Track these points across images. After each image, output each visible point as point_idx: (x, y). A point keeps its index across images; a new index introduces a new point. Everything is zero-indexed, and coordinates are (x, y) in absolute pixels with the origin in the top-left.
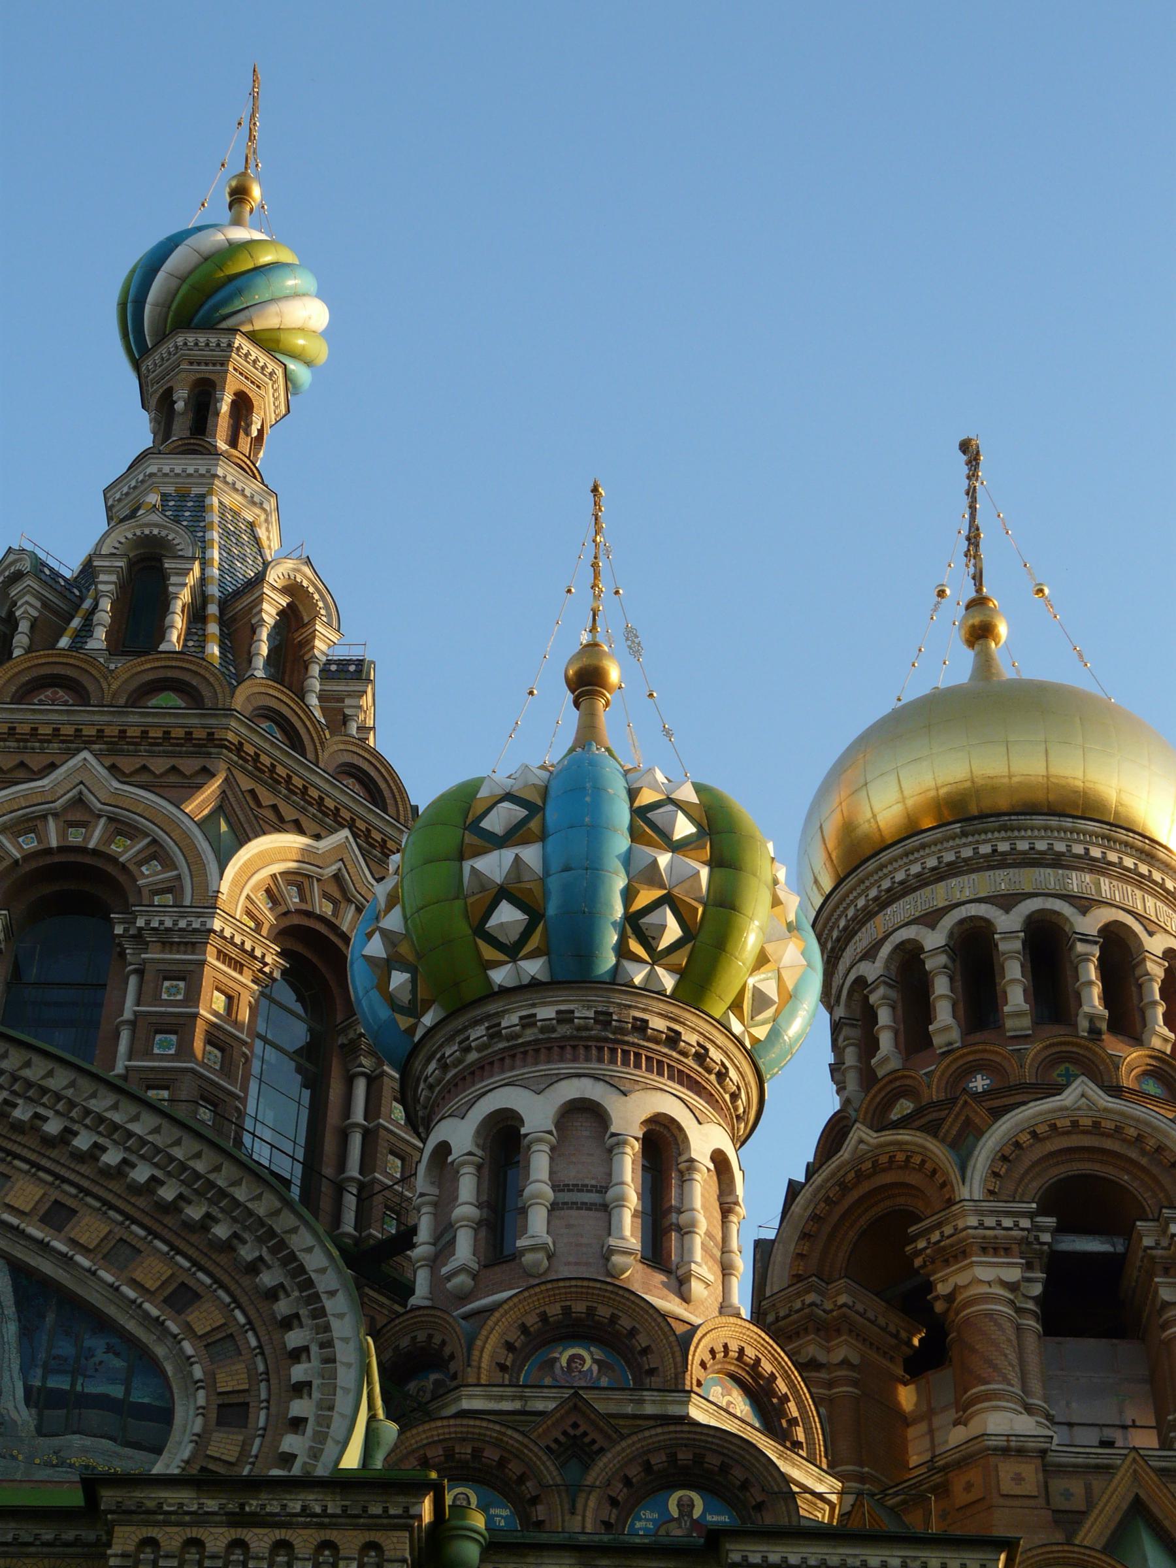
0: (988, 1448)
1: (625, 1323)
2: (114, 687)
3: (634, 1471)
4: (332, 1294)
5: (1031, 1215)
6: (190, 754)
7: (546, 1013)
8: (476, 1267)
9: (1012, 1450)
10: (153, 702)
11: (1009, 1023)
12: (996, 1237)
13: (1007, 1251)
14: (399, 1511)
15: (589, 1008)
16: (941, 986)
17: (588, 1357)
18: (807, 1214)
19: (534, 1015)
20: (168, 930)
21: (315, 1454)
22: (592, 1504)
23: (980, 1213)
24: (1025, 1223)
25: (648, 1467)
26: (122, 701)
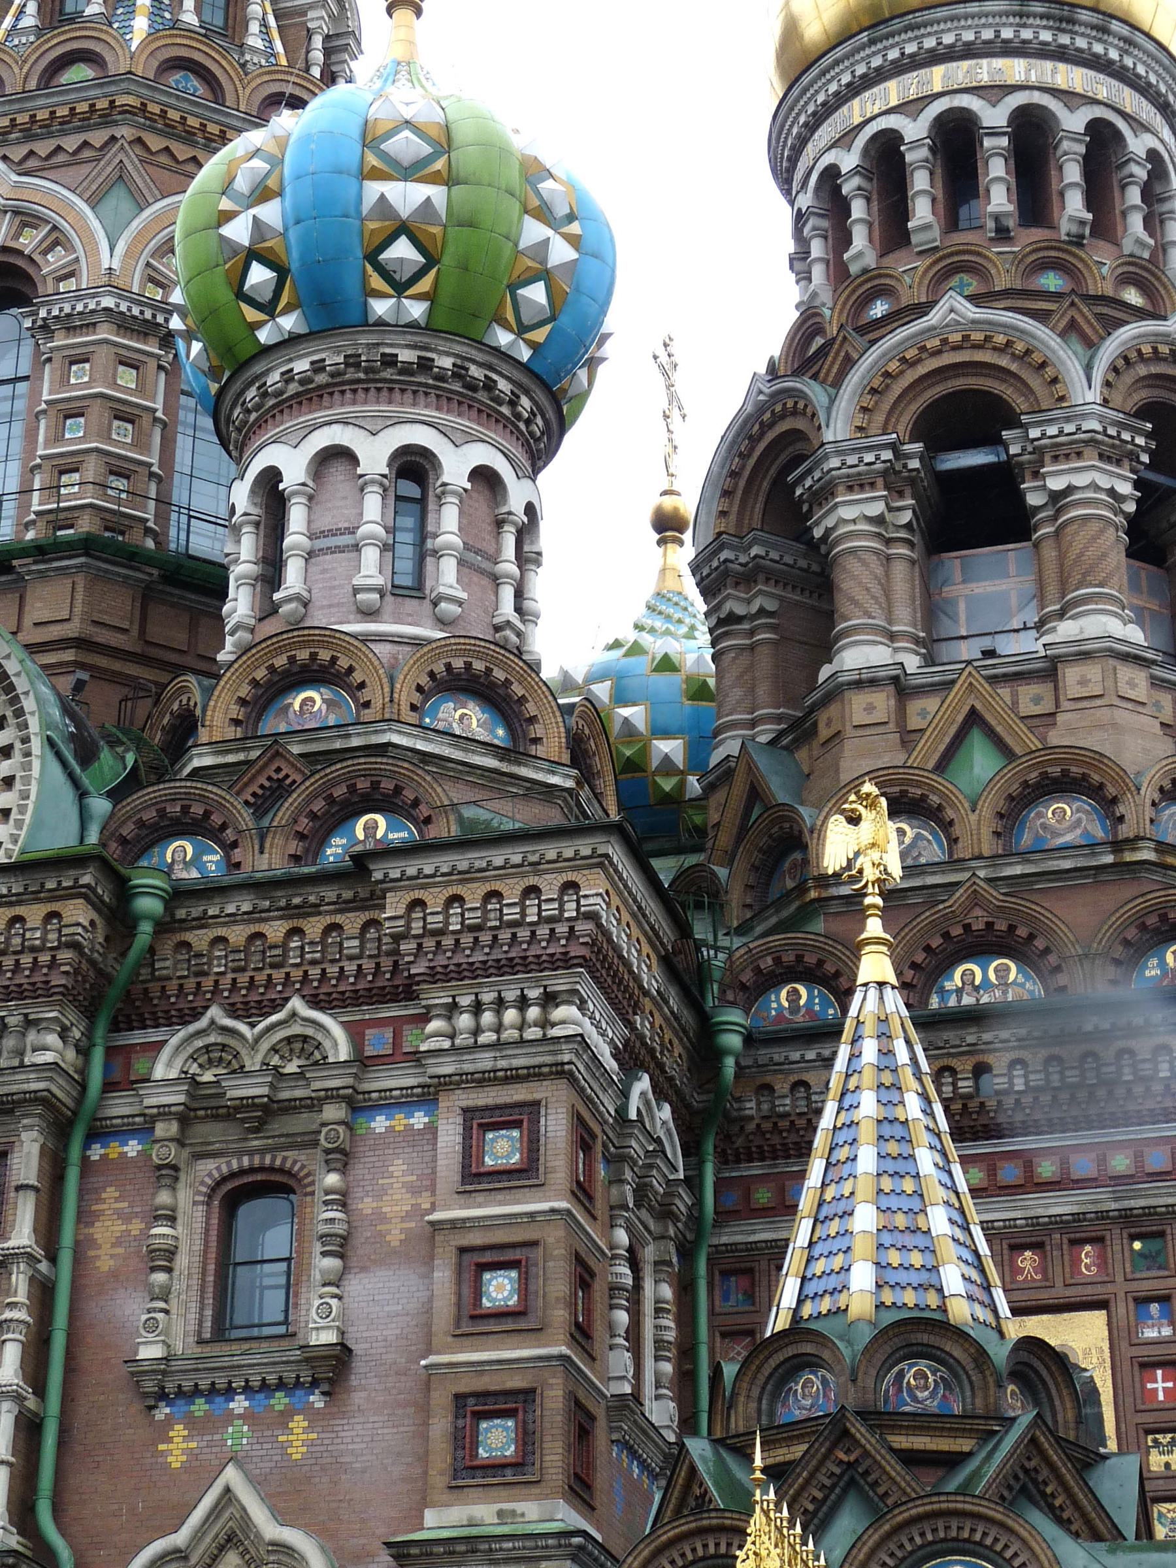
0: (842, 684)
1: (343, 662)
2: (25, 70)
3: (318, 806)
4: (26, 693)
5: (893, 446)
6: (98, 126)
7: (301, 366)
8: (253, 622)
9: (866, 682)
10: (63, 80)
11: (914, 239)
12: (859, 474)
13: (872, 485)
14: (71, 883)
15: (339, 353)
16: (858, 209)
17: (316, 696)
18: (725, 472)
19: (291, 370)
20: (68, 315)
21: (15, 842)
22: (279, 840)
23: (839, 453)
24: (887, 455)
25: (330, 800)
26: (32, 84)
